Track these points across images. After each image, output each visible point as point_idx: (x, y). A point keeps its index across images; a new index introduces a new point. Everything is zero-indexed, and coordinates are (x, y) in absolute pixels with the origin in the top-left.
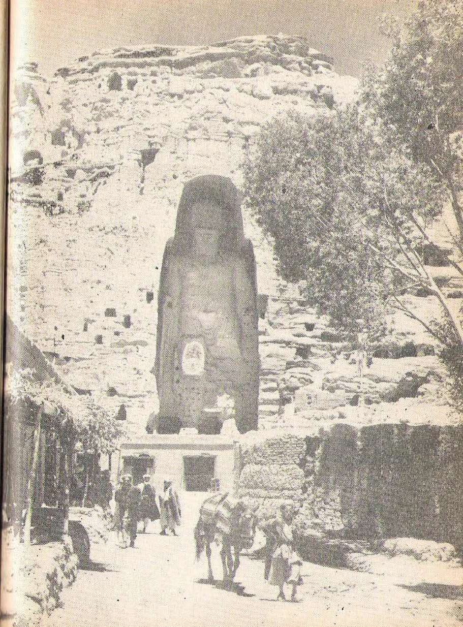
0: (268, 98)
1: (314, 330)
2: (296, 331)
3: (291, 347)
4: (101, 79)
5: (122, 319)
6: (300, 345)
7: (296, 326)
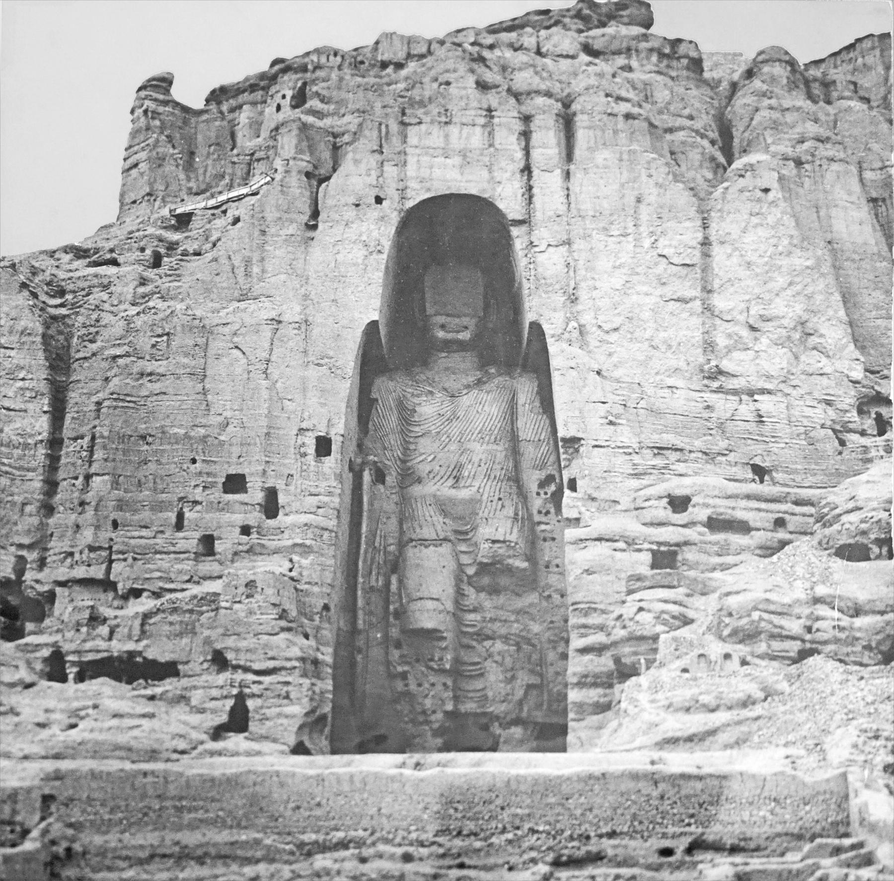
0: (573, 57)
1: (690, 509)
2: (648, 515)
3: (640, 550)
4: (280, 95)
5: (258, 496)
6: (659, 544)
7: (647, 504)
